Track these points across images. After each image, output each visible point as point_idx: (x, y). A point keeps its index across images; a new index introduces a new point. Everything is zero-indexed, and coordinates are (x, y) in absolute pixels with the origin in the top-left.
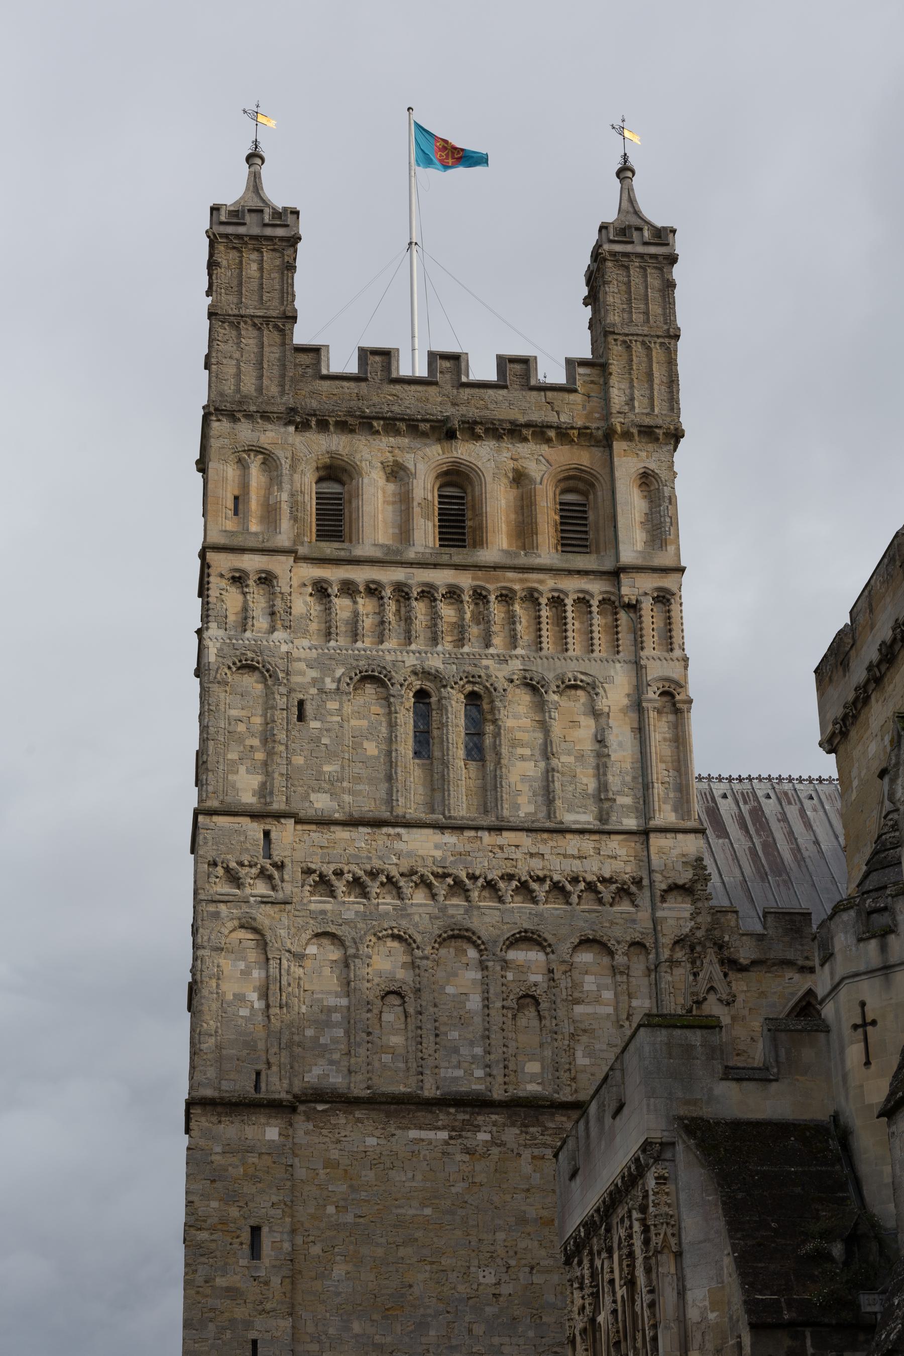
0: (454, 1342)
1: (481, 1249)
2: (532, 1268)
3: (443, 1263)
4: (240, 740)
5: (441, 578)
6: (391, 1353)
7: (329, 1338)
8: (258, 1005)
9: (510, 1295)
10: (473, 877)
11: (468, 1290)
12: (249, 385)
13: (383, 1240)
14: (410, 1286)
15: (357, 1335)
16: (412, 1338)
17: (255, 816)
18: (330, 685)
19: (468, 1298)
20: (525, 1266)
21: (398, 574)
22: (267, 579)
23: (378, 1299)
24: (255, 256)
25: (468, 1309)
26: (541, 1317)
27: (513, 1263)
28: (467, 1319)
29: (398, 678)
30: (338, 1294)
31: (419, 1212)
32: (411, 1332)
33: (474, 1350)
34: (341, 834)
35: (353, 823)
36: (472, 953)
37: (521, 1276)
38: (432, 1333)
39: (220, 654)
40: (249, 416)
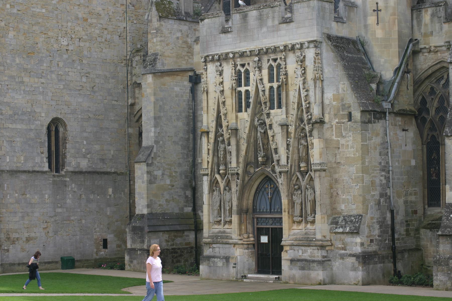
0: (52, 69)
1: (62, 29)
2: (80, 39)
3: (49, 34)
6: (30, 73)
7: (7, 64)
9: (72, 50)
11: (58, 47)
13: (27, 22)
14: (37, 43)
15: (17, 64)
16: (37, 67)
19: (58, 51)
20: (77, 38)
23: (25, 49)
25: (57, 55)
26: (82, 61)
27: (73, 36)
28: (57, 60)
30: (11, 45)
31: (40, 11)
32: (37, 64)
33: (59, 73)
37: (76, 42)
38: (45, 65)
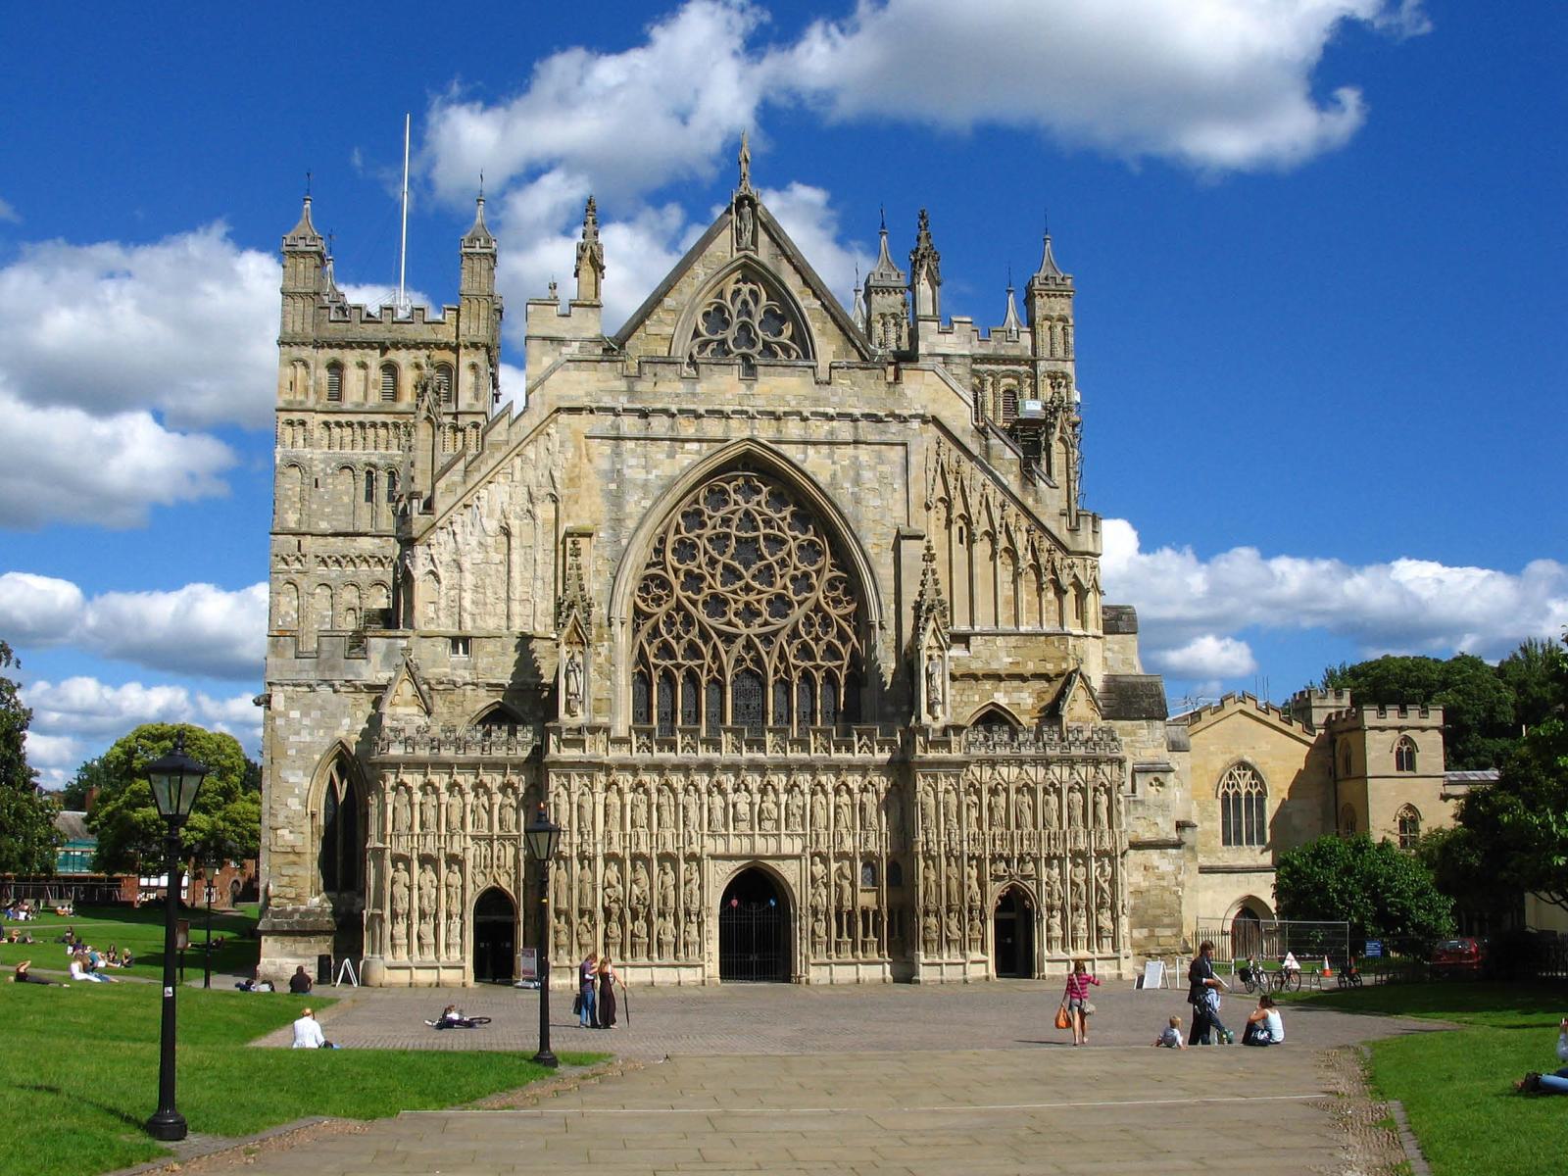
4: (288, 497)
5: (379, 418)
8: (295, 616)
10: (386, 558)
12: (298, 328)
17: (294, 534)
18: (329, 471)
21: (361, 418)
22: (303, 423)
24: (302, 260)
29: (358, 466)
34: (331, 540)
35: (336, 535)
36: (384, 590)
39: (282, 460)
40: (296, 344)
